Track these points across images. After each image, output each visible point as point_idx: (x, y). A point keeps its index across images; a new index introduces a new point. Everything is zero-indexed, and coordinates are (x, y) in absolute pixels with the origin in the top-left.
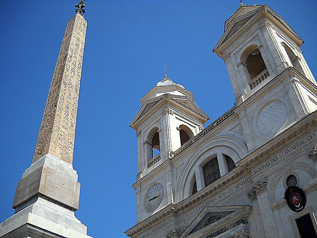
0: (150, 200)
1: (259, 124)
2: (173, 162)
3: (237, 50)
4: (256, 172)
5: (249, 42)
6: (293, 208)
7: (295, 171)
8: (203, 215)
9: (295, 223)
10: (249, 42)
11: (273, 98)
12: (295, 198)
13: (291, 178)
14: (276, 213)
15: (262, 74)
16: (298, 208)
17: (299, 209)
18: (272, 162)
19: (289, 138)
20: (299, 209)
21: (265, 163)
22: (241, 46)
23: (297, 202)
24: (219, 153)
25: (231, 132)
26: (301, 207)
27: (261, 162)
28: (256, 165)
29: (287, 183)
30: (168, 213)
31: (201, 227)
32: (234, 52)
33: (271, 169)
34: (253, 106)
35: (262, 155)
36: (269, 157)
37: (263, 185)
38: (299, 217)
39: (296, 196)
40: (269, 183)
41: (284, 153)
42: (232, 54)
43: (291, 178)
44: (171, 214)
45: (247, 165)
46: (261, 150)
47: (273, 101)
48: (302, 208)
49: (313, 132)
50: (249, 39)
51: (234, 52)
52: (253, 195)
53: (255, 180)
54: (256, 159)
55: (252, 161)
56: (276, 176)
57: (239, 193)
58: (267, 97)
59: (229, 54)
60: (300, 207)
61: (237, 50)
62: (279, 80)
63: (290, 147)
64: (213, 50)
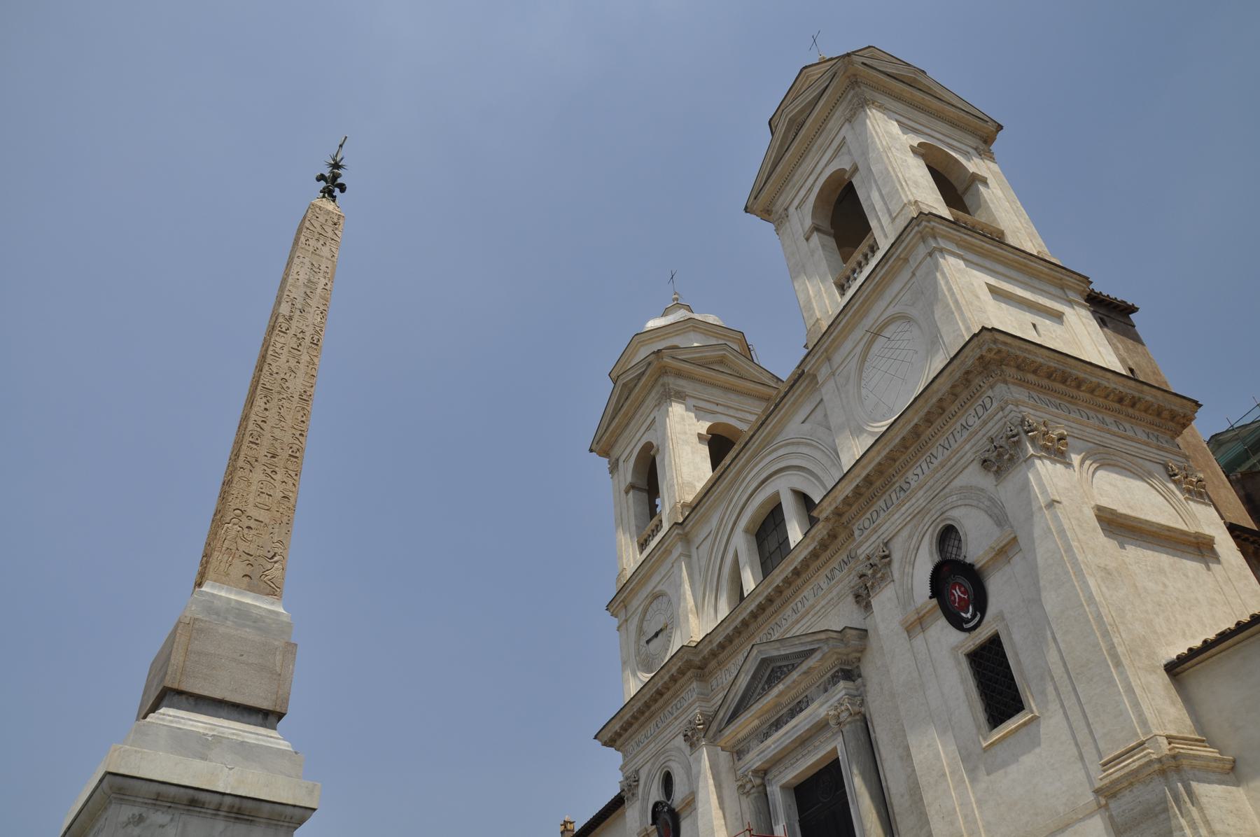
0: (648, 642)
1: (864, 392)
2: (687, 529)
3: (802, 193)
6: (957, 622)
7: (955, 513)
8: (751, 667)
9: (965, 664)
11: (891, 311)
12: (957, 593)
14: (919, 641)
15: (864, 247)
17: (972, 624)
19: (929, 420)
20: (972, 624)
21: (881, 503)
23: (963, 603)
24: (783, 487)
25: (807, 426)
26: (974, 616)
27: (871, 500)
30: (682, 672)
32: (796, 203)
33: (896, 516)
35: (868, 481)
36: (888, 484)
38: (972, 647)
39: (961, 585)
40: (896, 556)
42: (792, 210)
44: (689, 674)
46: (864, 468)
48: (977, 619)
49: (990, 393)
51: (796, 203)
53: (863, 551)
54: (857, 492)
55: (847, 502)
56: (910, 537)
57: (834, 593)
60: (974, 616)
61: (802, 193)
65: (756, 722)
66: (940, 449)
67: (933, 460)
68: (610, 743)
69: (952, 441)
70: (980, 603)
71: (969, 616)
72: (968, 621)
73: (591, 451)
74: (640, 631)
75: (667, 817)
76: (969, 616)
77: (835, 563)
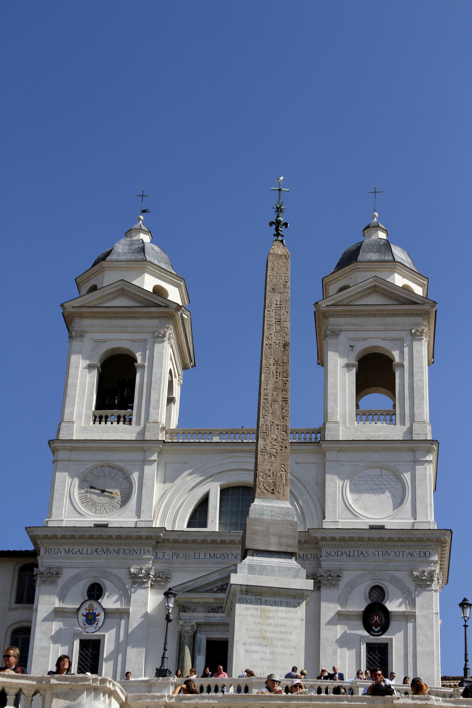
6: (368, 628)
12: (376, 618)
16: (374, 631)
17: (375, 634)
18: (359, 555)
20: (375, 634)
26: (378, 632)
29: (369, 593)
31: (212, 589)
41: (380, 553)
45: (323, 539)
49: (430, 551)
55: (333, 539)
59: (341, 331)
60: (378, 632)
62: (412, 448)
63: (393, 550)
64: (317, 303)
65: (212, 600)
66: (393, 553)
67: (387, 554)
69: (401, 555)
70: (384, 629)
71: (376, 630)
72: (374, 631)
73: (62, 305)
76: (376, 630)
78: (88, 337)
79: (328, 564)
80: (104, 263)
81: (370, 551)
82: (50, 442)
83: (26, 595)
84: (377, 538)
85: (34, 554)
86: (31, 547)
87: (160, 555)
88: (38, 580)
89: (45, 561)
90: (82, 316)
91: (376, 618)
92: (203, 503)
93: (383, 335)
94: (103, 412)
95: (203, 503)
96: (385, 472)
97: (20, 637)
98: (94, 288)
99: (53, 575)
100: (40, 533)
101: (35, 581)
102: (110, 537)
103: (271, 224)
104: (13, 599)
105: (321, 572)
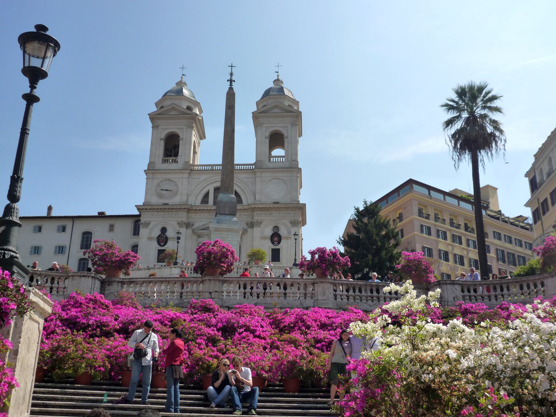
4: (257, 214)
5: (280, 127)
6: (273, 242)
10: (280, 127)
13: (276, 228)
19: (285, 208)
21: (264, 212)
22: (273, 125)
27: (262, 211)
28: (259, 211)
34: (268, 174)
37: (259, 223)
43: (276, 228)
45: (255, 208)
47: (282, 180)
50: (281, 125)
51: (266, 125)
52: (252, 225)
58: (278, 175)
61: (269, 125)
68: (138, 209)
74: (158, 185)
75: (165, 239)
77: (243, 213)
78: (160, 127)
79: (256, 218)
80: (166, 97)
81: (273, 212)
82: (145, 171)
83: (136, 232)
84: (277, 206)
85: (139, 216)
86: (138, 213)
87: (190, 215)
88: (141, 226)
89: (143, 219)
90: (157, 118)
91: (276, 239)
92: (207, 195)
93: (281, 125)
94: (167, 158)
95: (207, 195)
96: (280, 181)
97: (135, 249)
98: (162, 107)
99: (147, 224)
100: (141, 208)
101: (139, 227)
102: (169, 209)
103: (228, 80)
104: (132, 234)
105: (254, 221)
